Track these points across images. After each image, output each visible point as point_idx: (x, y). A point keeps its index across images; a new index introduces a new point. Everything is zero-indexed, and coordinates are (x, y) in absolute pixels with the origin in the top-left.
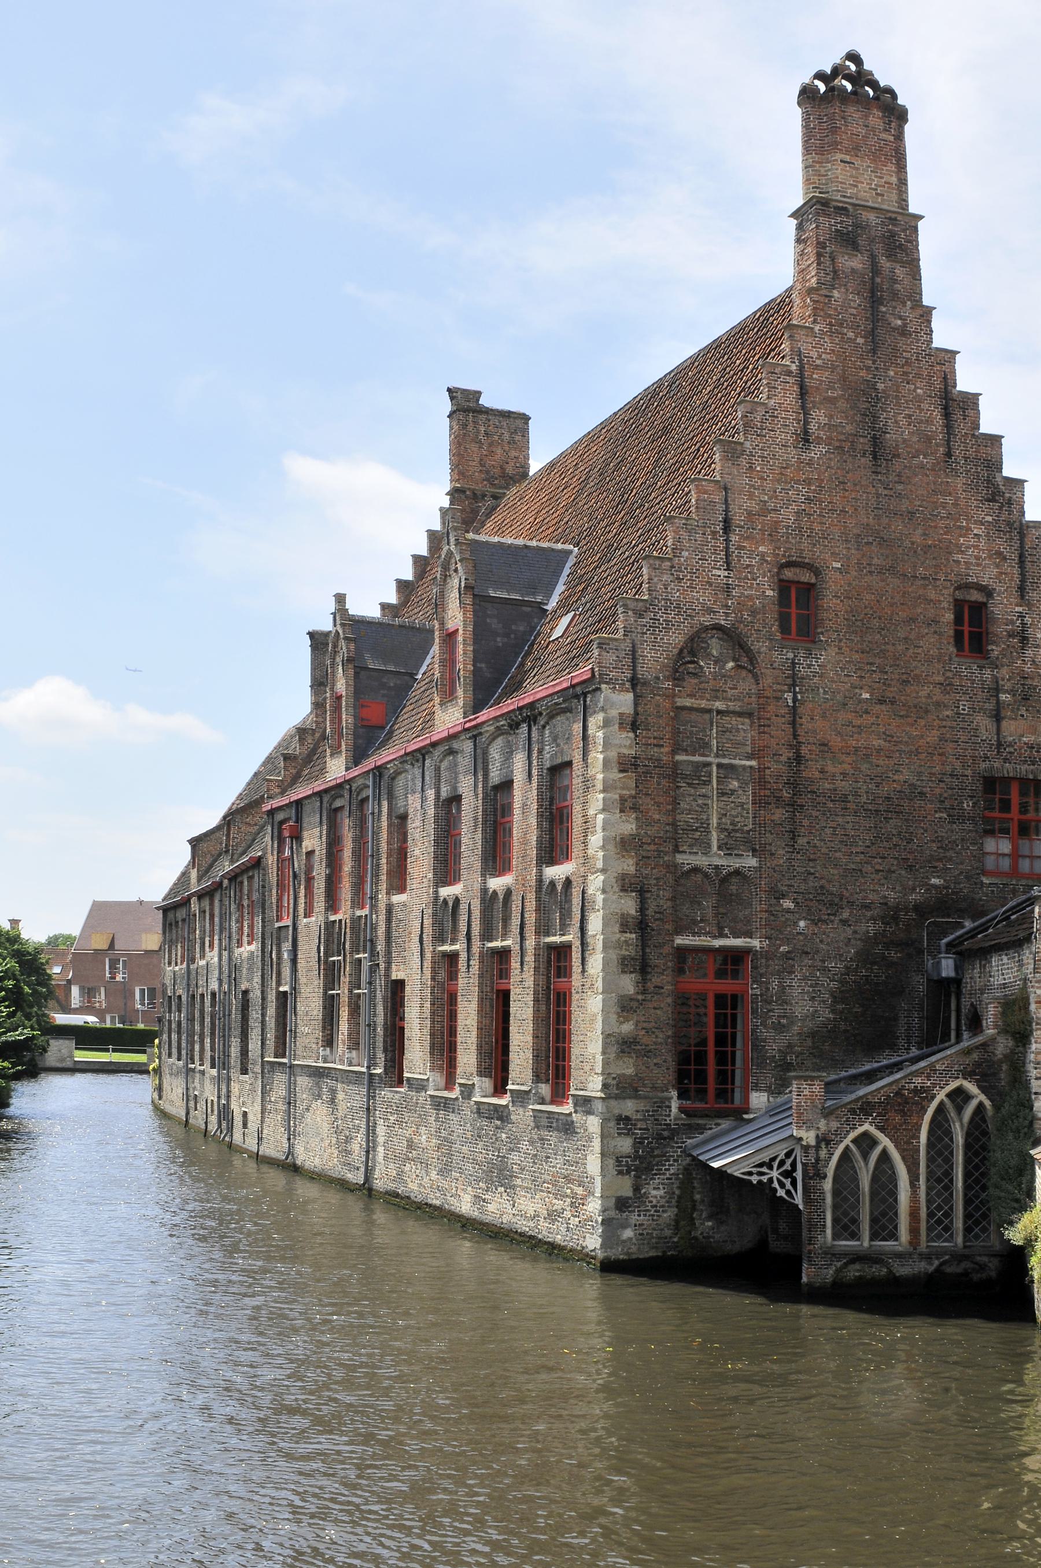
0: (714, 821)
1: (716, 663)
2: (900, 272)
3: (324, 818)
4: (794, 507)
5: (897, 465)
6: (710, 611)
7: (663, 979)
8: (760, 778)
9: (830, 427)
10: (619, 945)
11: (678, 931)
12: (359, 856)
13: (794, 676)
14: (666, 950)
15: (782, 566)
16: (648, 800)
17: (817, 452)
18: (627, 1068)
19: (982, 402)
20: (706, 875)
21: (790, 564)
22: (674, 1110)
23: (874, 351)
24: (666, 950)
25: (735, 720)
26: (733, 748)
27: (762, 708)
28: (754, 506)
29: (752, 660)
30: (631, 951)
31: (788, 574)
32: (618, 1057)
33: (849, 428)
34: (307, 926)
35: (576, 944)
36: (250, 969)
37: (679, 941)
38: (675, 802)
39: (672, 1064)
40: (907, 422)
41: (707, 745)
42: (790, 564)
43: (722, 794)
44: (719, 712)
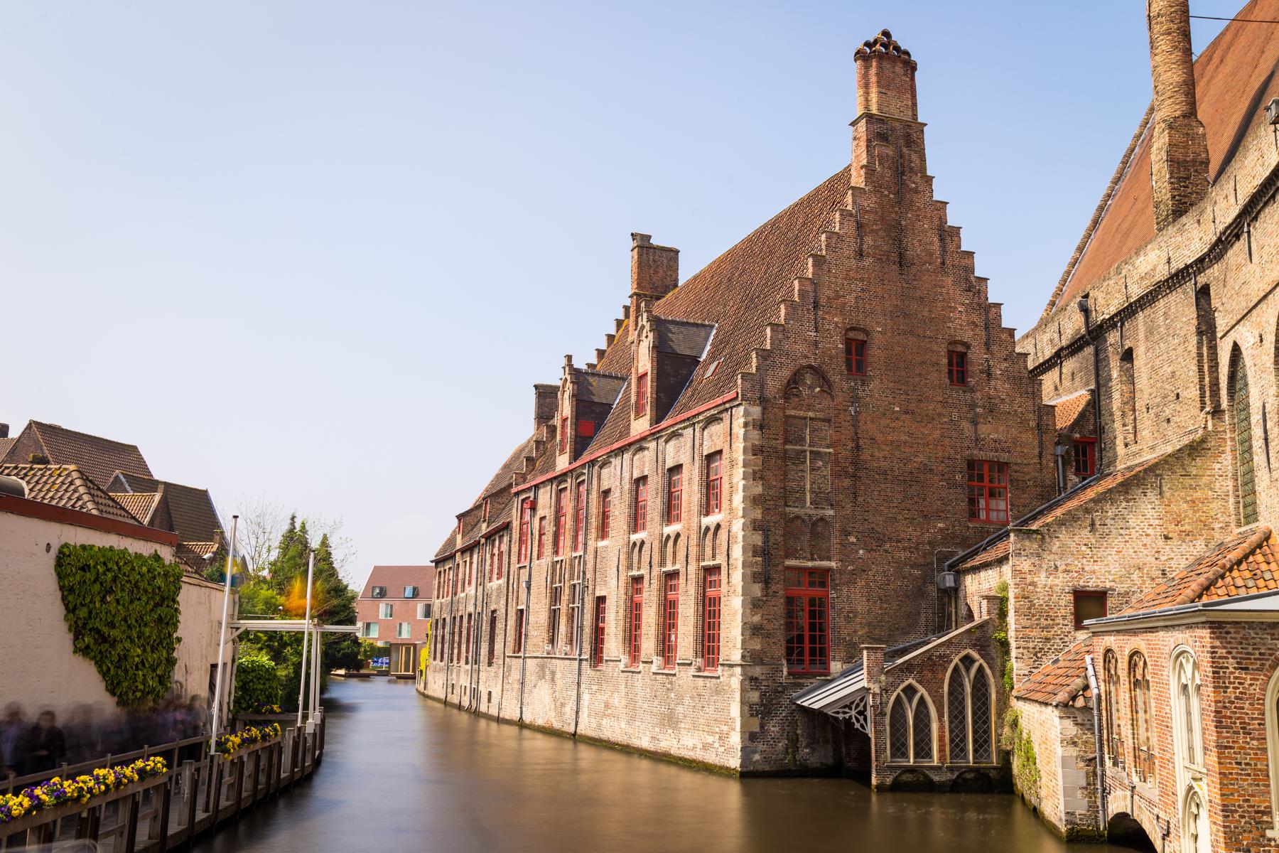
0: (808, 486)
2: (914, 157)
4: (854, 294)
5: (913, 270)
7: (779, 588)
9: (876, 247)
11: (787, 556)
12: (577, 519)
15: (848, 330)
16: (769, 473)
17: (868, 262)
18: (756, 645)
20: (803, 521)
21: (852, 329)
22: (785, 673)
24: (780, 568)
27: (836, 416)
28: (830, 293)
30: (758, 569)
31: (851, 335)
35: (724, 565)
36: (498, 596)
38: (785, 475)
39: (783, 643)
40: (921, 243)
41: (804, 439)
42: (852, 329)
43: (812, 469)
44: (811, 419)
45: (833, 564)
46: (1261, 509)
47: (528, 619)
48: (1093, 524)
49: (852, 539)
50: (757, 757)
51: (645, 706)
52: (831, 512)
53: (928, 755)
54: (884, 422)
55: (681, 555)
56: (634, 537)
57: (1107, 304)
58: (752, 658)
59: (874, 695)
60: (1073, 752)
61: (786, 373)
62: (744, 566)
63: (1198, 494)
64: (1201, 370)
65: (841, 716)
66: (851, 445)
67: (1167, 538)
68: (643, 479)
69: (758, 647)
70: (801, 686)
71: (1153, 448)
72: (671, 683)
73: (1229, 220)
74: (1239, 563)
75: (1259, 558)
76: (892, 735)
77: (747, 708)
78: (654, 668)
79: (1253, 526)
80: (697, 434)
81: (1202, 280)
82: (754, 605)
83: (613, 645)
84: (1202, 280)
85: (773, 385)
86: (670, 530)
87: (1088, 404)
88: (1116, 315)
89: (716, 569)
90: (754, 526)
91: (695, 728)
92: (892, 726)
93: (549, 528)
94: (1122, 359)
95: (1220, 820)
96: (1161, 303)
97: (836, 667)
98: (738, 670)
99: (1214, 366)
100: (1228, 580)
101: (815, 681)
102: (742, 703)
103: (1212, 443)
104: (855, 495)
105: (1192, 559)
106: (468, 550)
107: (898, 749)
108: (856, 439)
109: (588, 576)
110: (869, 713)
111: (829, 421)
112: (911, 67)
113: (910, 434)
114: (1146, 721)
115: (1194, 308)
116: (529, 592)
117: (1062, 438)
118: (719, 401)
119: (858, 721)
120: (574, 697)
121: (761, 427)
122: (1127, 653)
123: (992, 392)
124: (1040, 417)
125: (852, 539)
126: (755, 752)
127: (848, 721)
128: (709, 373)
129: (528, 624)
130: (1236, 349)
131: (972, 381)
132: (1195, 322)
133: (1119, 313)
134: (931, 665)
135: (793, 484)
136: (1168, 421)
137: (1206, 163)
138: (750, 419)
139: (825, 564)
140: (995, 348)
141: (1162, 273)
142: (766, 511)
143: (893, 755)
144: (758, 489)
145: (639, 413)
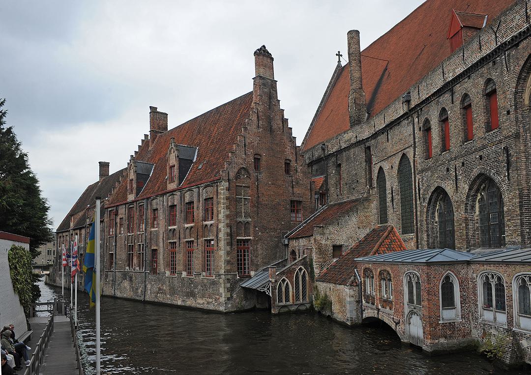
3: (127, 210)
7: (235, 247)
10: (227, 239)
14: (236, 240)
25: (246, 188)
26: (247, 195)
31: (256, 156)
32: (227, 265)
33: (266, 125)
34: (120, 236)
45: (251, 238)
47: (116, 257)
48: (338, 224)
49: (257, 229)
51: (179, 289)
52: (250, 220)
53: (289, 301)
56: (169, 228)
58: (227, 272)
60: (352, 299)
61: (236, 170)
64: (366, 172)
67: (359, 228)
68: (173, 207)
69: (229, 268)
70: (243, 280)
72: (191, 281)
77: (226, 289)
78: (183, 276)
81: (367, 144)
82: (228, 253)
83: (161, 267)
84: (367, 144)
85: (232, 175)
86: (186, 226)
88: (335, 152)
91: (203, 297)
93: (126, 223)
94: (336, 167)
95: (428, 320)
96: (352, 150)
97: (252, 273)
99: (370, 173)
101: (247, 279)
104: (258, 214)
105: (366, 235)
106: (80, 229)
107: (280, 300)
109: (147, 241)
110: (270, 289)
111: (249, 187)
114: (386, 291)
116: (116, 248)
119: (267, 291)
120: (143, 285)
122: (379, 270)
124: (311, 185)
127: (264, 292)
129: (116, 259)
130: (381, 168)
134: (289, 272)
135: (238, 210)
136: (354, 189)
140: (298, 162)
141: (353, 141)
144: (228, 213)
145: (172, 181)
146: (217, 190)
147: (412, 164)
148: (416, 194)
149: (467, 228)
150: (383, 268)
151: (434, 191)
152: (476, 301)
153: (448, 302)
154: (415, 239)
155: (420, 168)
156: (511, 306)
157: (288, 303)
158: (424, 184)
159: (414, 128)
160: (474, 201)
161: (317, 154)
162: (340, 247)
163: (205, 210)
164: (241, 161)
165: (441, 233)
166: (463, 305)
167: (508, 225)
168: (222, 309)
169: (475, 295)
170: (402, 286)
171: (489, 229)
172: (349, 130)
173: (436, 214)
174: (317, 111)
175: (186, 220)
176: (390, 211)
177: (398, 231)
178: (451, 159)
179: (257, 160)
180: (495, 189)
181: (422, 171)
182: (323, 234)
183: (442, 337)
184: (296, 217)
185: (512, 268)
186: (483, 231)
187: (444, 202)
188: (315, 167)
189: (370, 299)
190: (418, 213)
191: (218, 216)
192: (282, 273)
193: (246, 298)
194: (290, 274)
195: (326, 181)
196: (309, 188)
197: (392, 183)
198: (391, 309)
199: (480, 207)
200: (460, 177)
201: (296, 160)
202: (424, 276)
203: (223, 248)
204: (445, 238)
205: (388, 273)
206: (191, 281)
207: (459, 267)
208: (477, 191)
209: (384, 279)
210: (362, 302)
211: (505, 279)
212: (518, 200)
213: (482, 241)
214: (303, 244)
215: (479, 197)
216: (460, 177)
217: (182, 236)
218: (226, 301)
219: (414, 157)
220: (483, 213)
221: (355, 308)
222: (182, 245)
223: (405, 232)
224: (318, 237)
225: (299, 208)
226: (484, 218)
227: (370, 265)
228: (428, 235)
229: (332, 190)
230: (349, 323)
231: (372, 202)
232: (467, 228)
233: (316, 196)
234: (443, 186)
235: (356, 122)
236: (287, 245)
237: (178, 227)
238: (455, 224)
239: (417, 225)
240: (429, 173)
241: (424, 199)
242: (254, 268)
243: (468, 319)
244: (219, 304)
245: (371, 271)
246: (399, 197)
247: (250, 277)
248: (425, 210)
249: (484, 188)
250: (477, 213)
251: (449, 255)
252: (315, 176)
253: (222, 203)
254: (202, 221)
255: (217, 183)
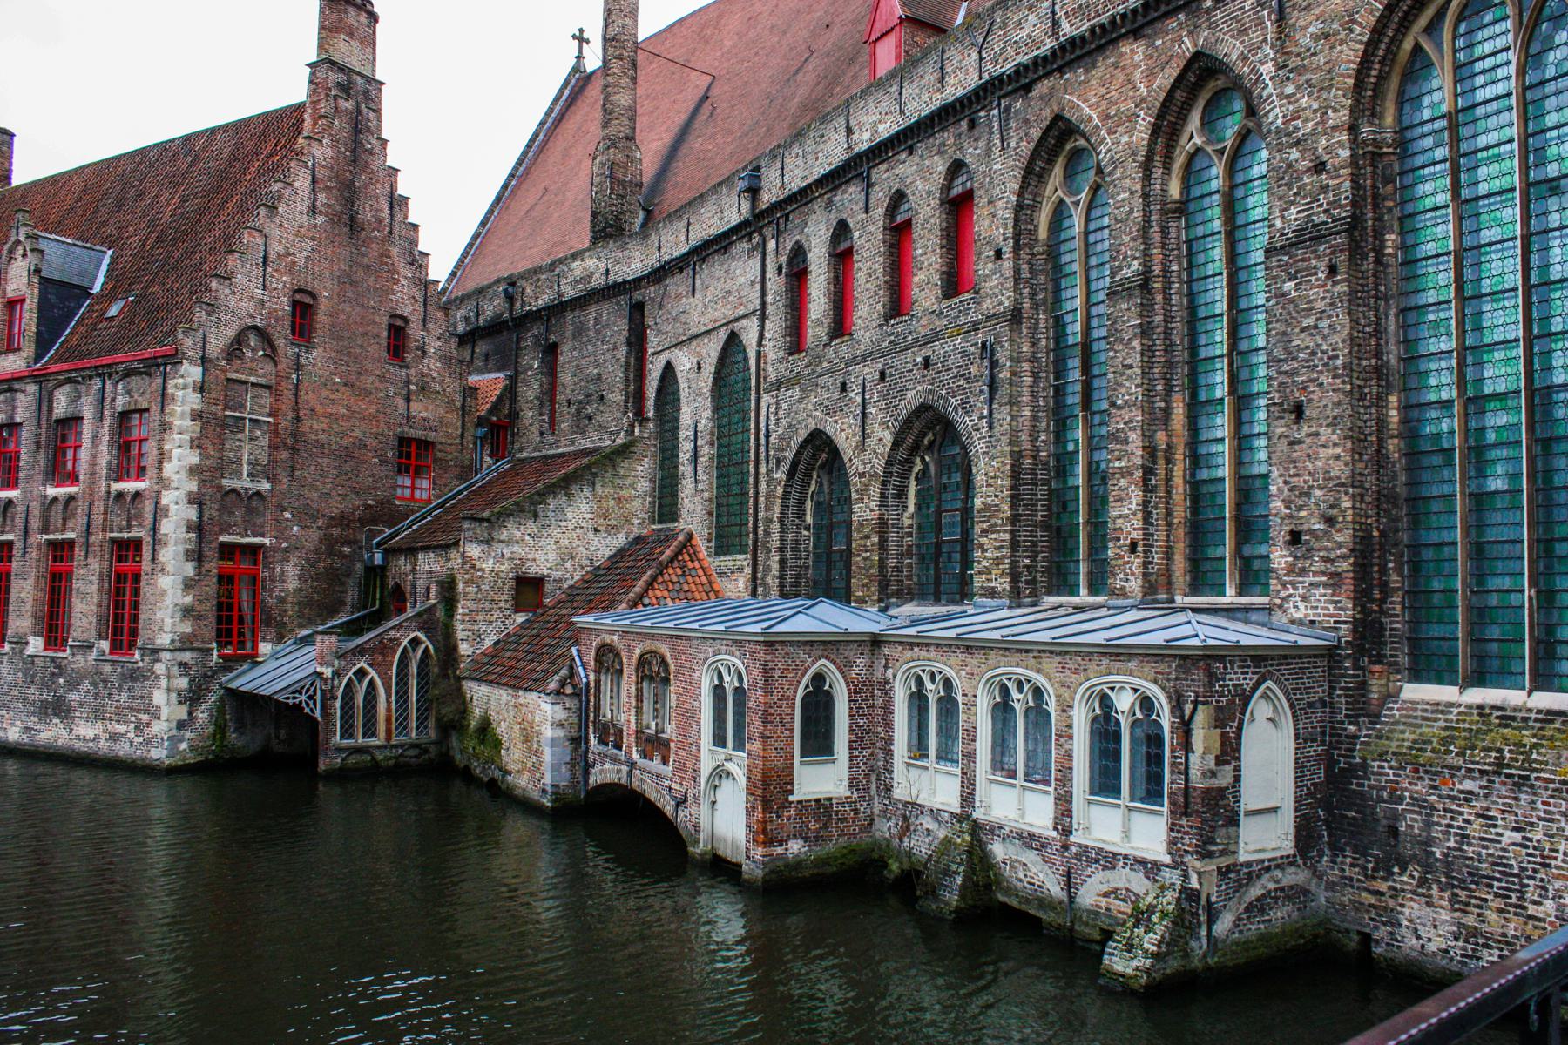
1: (253, 351)
5: (363, 235)
6: (252, 316)
7: (213, 566)
8: (274, 431)
13: (298, 364)
14: (214, 545)
15: (296, 291)
17: (321, 219)
18: (186, 628)
19: (411, 203)
20: (239, 494)
21: (299, 291)
23: (354, 161)
25: (260, 391)
27: (278, 383)
29: (274, 348)
30: (192, 546)
31: (298, 297)
33: (338, 208)
35: (148, 540)
37: (221, 538)
44: (253, 384)
45: (267, 541)
46: (684, 513)
48: (536, 516)
49: (288, 515)
50: (184, 746)
53: (374, 734)
54: (325, 393)
55: (81, 520)
57: (538, 298)
59: (326, 680)
60: (560, 733)
61: (230, 333)
62: (176, 543)
63: (624, 492)
64: (627, 378)
65: (291, 701)
66: (291, 415)
69: (189, 630)
70: (231, 669)
71: (572, 442)
72: (59, 667)
73: (676, 254)
74: (672, 560)
75: (687, 558)
76: (342, 718)
77: (174, 695)
79: (671, 525)
80: (109, 387)
82: (188, 585)
85: (216, 345)
87: (505, 389)
89: (137, 544)
90: (193, 499)
91: (96, 716)
92: (342, 708)
94: (544, 352)
95: (759, 792)
96: (593, 308)
97: (265, 648)
98: (166, 656)
100: (666, 577)
102: (169, 690)
103: (638, 448)
104: (293, 469)
108: (296, 410)
112: (374, 18)
113: (349, 408)
114: (656, 710)
115: (626, 321)
117: (481, 422)
118: (148, 353)
121: (202, 390)
122: (638, 651)
123: (425, 370)
125: (288, 515)
126: (181, 741)
127: (298, 707)
128: (113, 311)
130: (669, 368)
131: (409, 357)
132: (626, 333)
133: (546, 308)
136: (590, 418)
137: (640, 185)
138: (189, 380)
139: (257, 540)
140: (430, 326)
141: (598, 281)
142: (202, 482)
143: (342, 737)
144: (194, 458)
146: (164, 388)
147: (752, 362)
148: (757, 446)
149: (882, 547)
150: (650, 645)
151: (806, 442)
152: (890, 741)
153: (818, 742)
154: (748, 571)
155: (772, 376)
156: (970, 756)
157: (373, 741)
158: (783, 417)
159: (763, 266)
160: (905, 476)
161: (492, 308)
162: (538, 583)
163: (119, 448)
164: (248, 306)
165: (817, 557)
166: (856, 753)
167: (981, 546)
168: (158, 754)
169: (889, 725)
170: (697, 699)
171: (938, 553)
172: (589, 249)
173: (809, 505)
174: (505, 186)
175: (58, 470)
176: (687, 488)
177: (702, 545)
178: (855, 360)
179: (303, 312)
180: (957, 450)
181: (779, 385)
182: (488, 541)
183: (795, 837)
184: (413, 488)
185: (980, 655)
186: (922, 558)
187: (830, 472)
188: (482, 348)
189: (610, 734)
190: (762, 500)
191: (160, 468)
192: (360, 651)
193: (240, 727)
194: (383, 654)
195: (511, 391)
196: (458, 404)
197: (696, 411)
198: (665, 761)
199: (919, 494)
200: (873, 410)
201: (424, 320)
202: (757, 672)
203: (170, 568)
204: (829, 571)
205: (664, 662)
206: (59, 668)
207: (850, 652)
208: (915, 449)
209: (651, 678)
210: (587, 741)
211: (959, 684)
212: (1007, 482)
213: (920, 584)
214: (427, 568)
215: (918, 467)
216: (873, 410)
217: (35, 524)
218: (174, 732)
219: (760, 344)
220: (924, 511)
221: (568, 759)
222: (33, 553)
223: (722, 548)
224: (474, 551)
225: (422, 462)
226: (929, 521)
227: (615, 638)
228: (783, 562)
229: (528, 416)
230: (547, 802)
231: (639, 461)
232: (882, 547)
233: (481, 431)
234: (829, 429)
235: (608, 230)
236: (383, 568)
237: (24, 495)
238: (855, 535)
239: (755, 532)
240: (797, 393)
241: (778, 462)
242: (272, 633)
243: (867, 790)
244: (148, 741)
245: (618, 655)
246: (714, 451)
247: (253, 659)
248: (780, 490)
249: (932, 443)
250: (911, 509)
251: (827, 617)
252: (481, 372)
253: (176, 430)
254: (108, 478)
255: (166, 365)
